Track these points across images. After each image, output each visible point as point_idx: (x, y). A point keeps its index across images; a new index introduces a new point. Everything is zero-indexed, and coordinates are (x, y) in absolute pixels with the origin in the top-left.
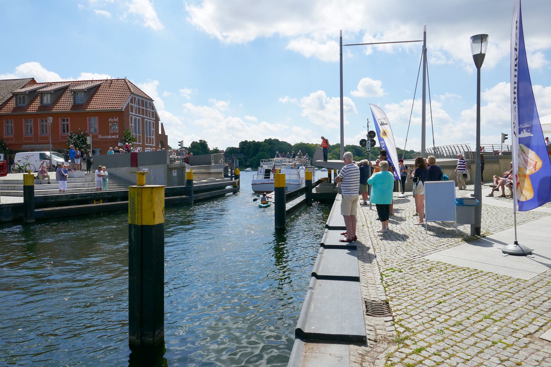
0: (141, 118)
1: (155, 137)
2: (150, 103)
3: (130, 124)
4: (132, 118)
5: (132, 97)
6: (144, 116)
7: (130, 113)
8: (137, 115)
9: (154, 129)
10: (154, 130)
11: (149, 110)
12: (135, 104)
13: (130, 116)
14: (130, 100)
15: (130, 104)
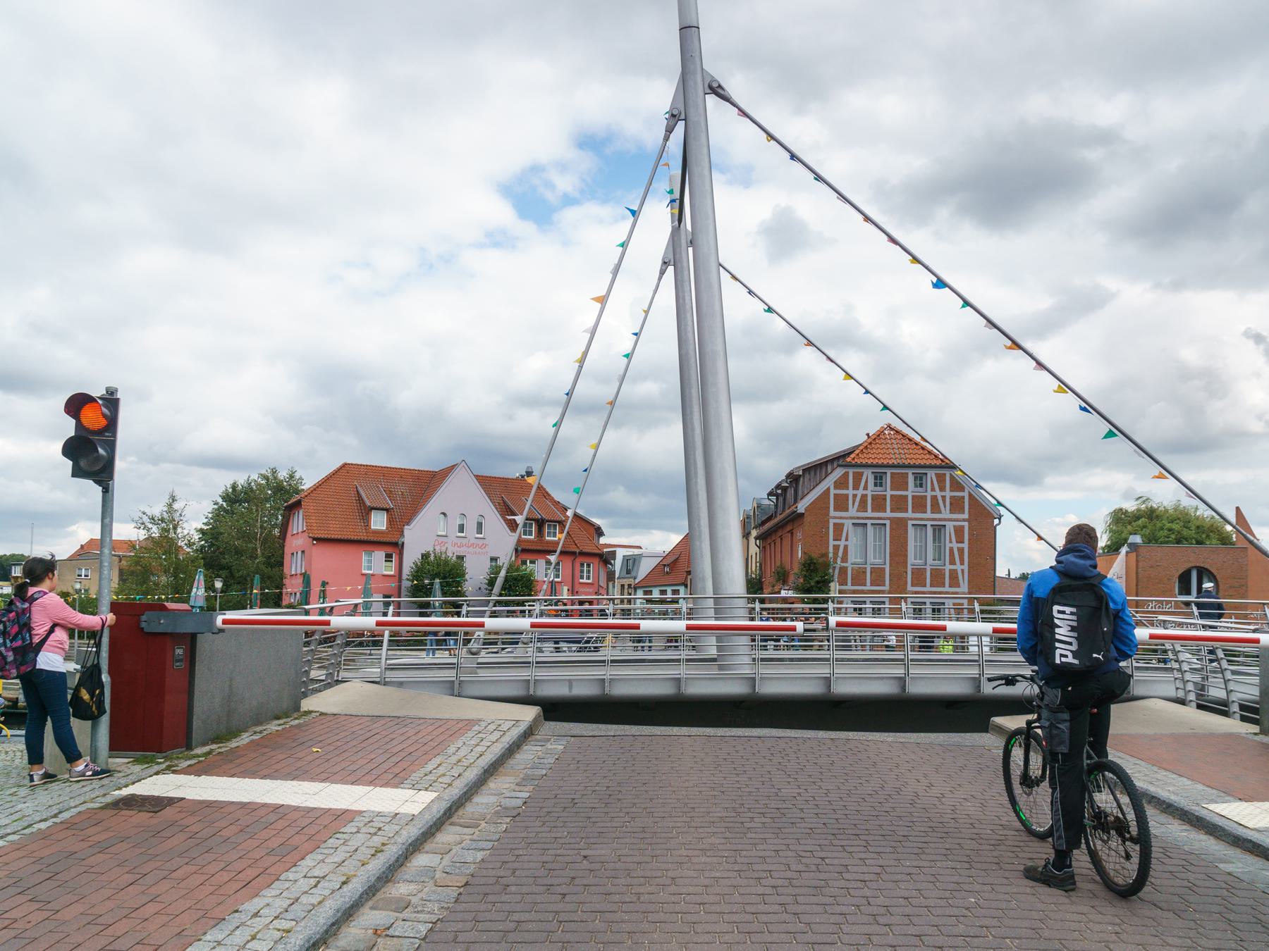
0: (888, 522)
1: (966, 567)
2: (941, 479)
3: (832, 543)
4: (839, 528)
5: (846, 474)
6: (910, 514)
7: (832, 513)
8: (870, 514)
9: (965, 545)
10: (961, 551)
11: (938, 493)
12: (856, 487)
13: (832, 522)
14: (835, 482)
15: (832, 492)
